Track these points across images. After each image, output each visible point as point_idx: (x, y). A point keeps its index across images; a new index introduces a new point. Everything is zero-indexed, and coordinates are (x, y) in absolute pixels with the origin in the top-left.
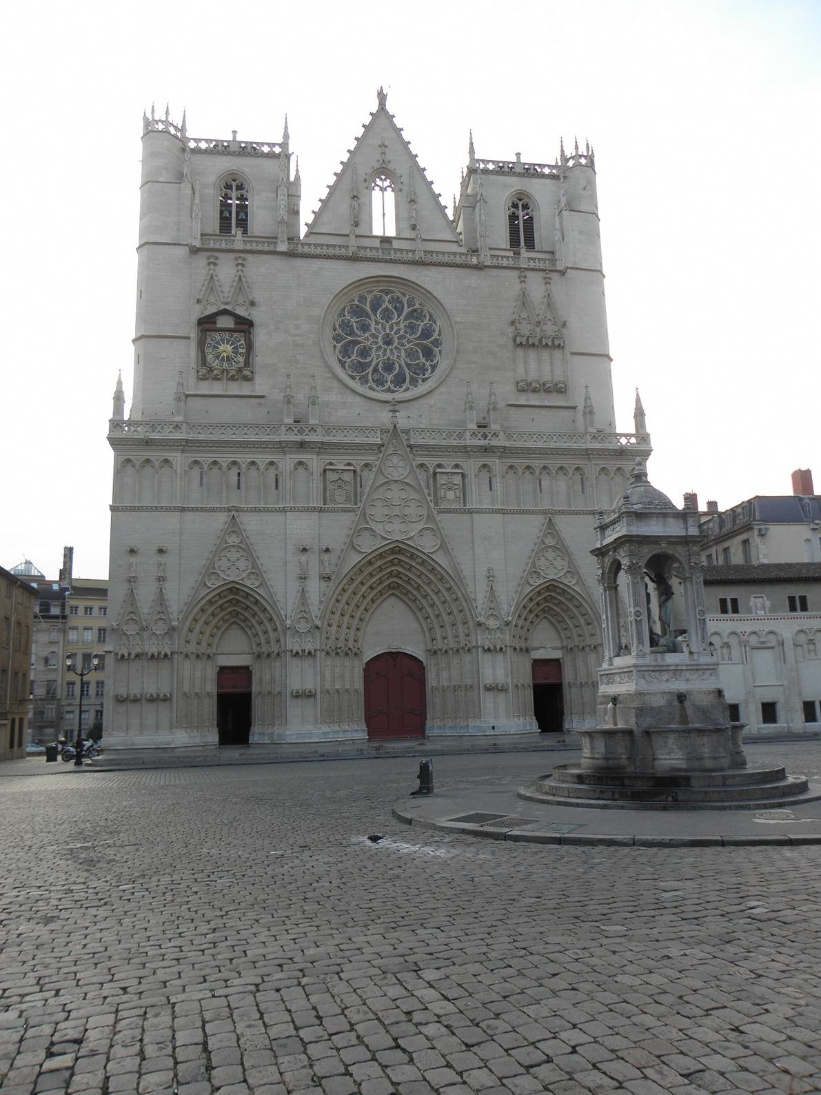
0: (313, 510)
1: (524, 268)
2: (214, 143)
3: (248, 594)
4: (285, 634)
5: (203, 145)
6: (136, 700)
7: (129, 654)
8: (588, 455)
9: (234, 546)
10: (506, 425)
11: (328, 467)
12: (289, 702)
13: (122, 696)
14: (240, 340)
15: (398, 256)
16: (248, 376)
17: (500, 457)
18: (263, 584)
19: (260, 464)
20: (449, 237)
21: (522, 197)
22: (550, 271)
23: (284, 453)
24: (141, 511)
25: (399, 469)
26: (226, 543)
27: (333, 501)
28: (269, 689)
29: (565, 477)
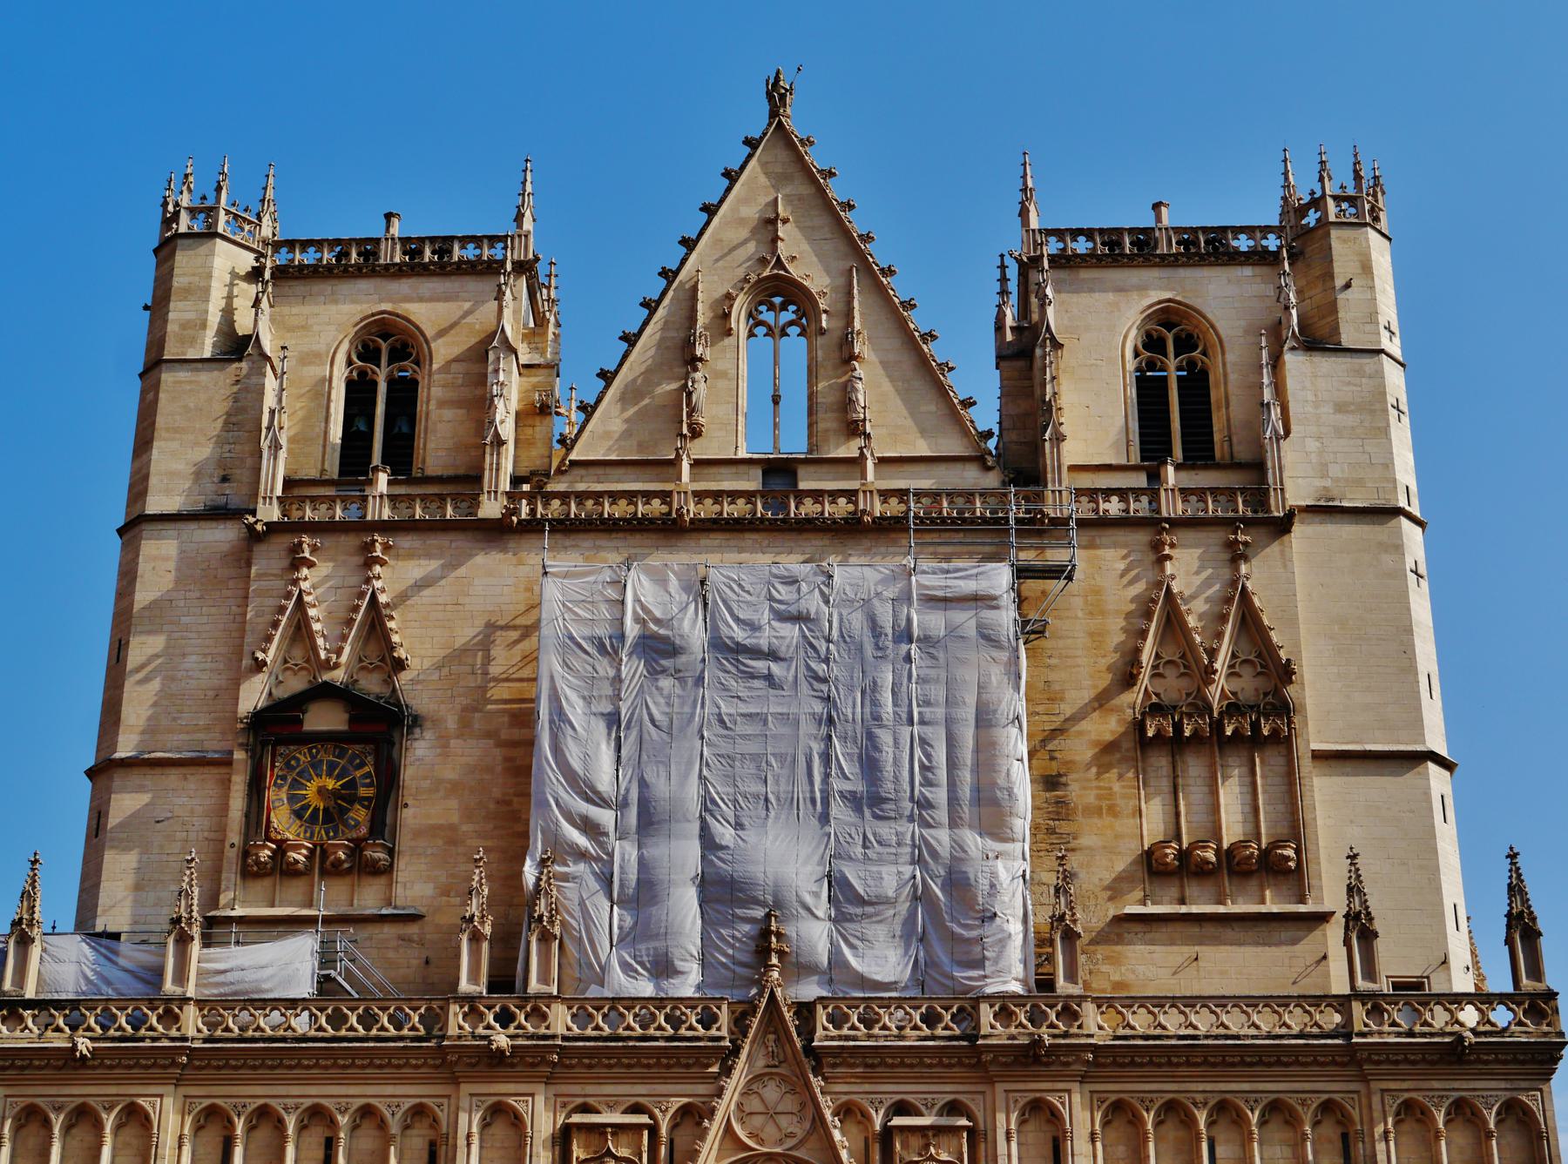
1: (1167, 520)
2: (338, 249)
5: (309, 257)
8: (1360, 1064)
10: (1116, 977)
11: (577, 1118)
14: (362, 765)
15: (809, 508)
16: (376, 861)
17: (1083, 1079)
19: (387, 1114)
20: (953, 445)
21: (1175, 319)
22: (1249, 523)
23: (455, 1081)
25: (783, 1121)
29: (1288, 1134)
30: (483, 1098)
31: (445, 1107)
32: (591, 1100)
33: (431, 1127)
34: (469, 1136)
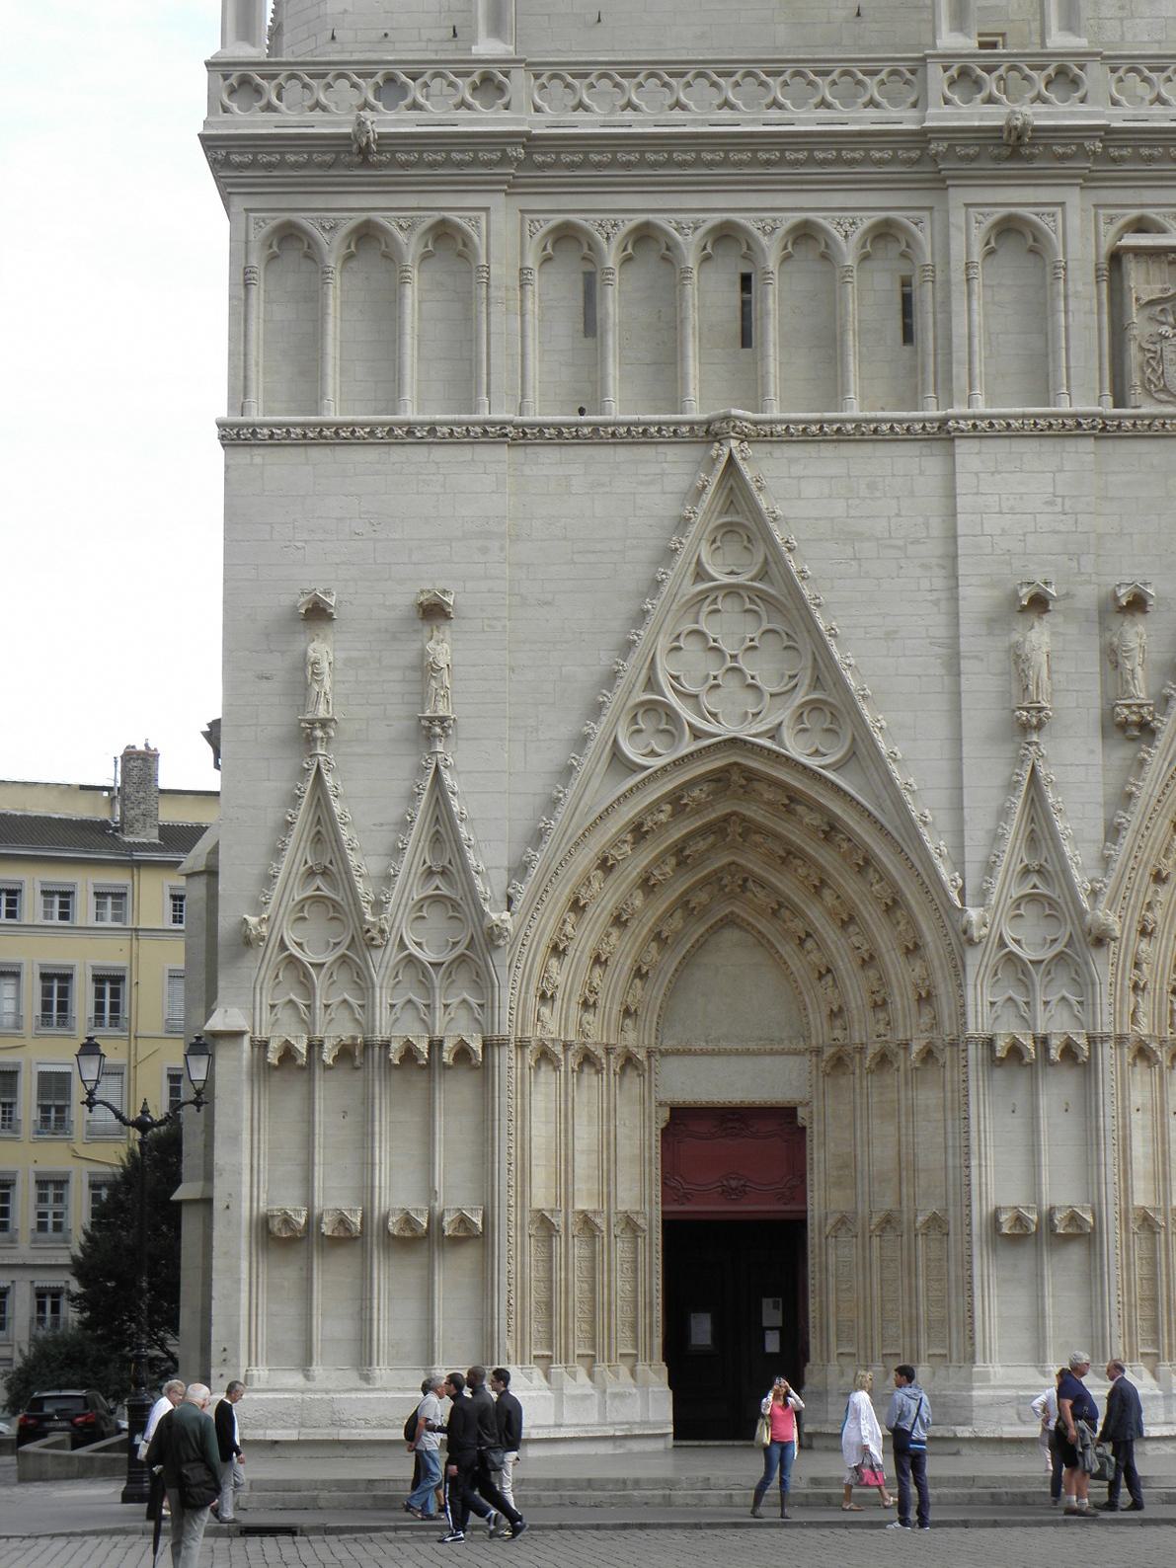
0: (1074, 429)
3: (794, 798)
4: (958, 970)
6: (346, 1239)
7: (314, 1047)
9: (732, 591)
11: (1132, 240)
12: (984, 1268)
13: (287, 1221)
18: (862, 752)
19: (840, 238)
23: (940, 183)
24: (346, 443)
26: (701, 574)
27: (1155, 388)
28: (888, 1202)
30: (986, 210)
31: (927, 224)
32: (1150, 212)
33: (904, 255)
34: (968, 266)
